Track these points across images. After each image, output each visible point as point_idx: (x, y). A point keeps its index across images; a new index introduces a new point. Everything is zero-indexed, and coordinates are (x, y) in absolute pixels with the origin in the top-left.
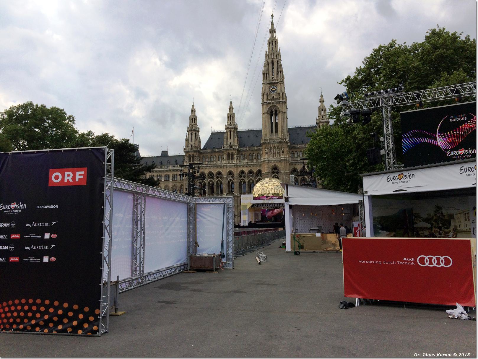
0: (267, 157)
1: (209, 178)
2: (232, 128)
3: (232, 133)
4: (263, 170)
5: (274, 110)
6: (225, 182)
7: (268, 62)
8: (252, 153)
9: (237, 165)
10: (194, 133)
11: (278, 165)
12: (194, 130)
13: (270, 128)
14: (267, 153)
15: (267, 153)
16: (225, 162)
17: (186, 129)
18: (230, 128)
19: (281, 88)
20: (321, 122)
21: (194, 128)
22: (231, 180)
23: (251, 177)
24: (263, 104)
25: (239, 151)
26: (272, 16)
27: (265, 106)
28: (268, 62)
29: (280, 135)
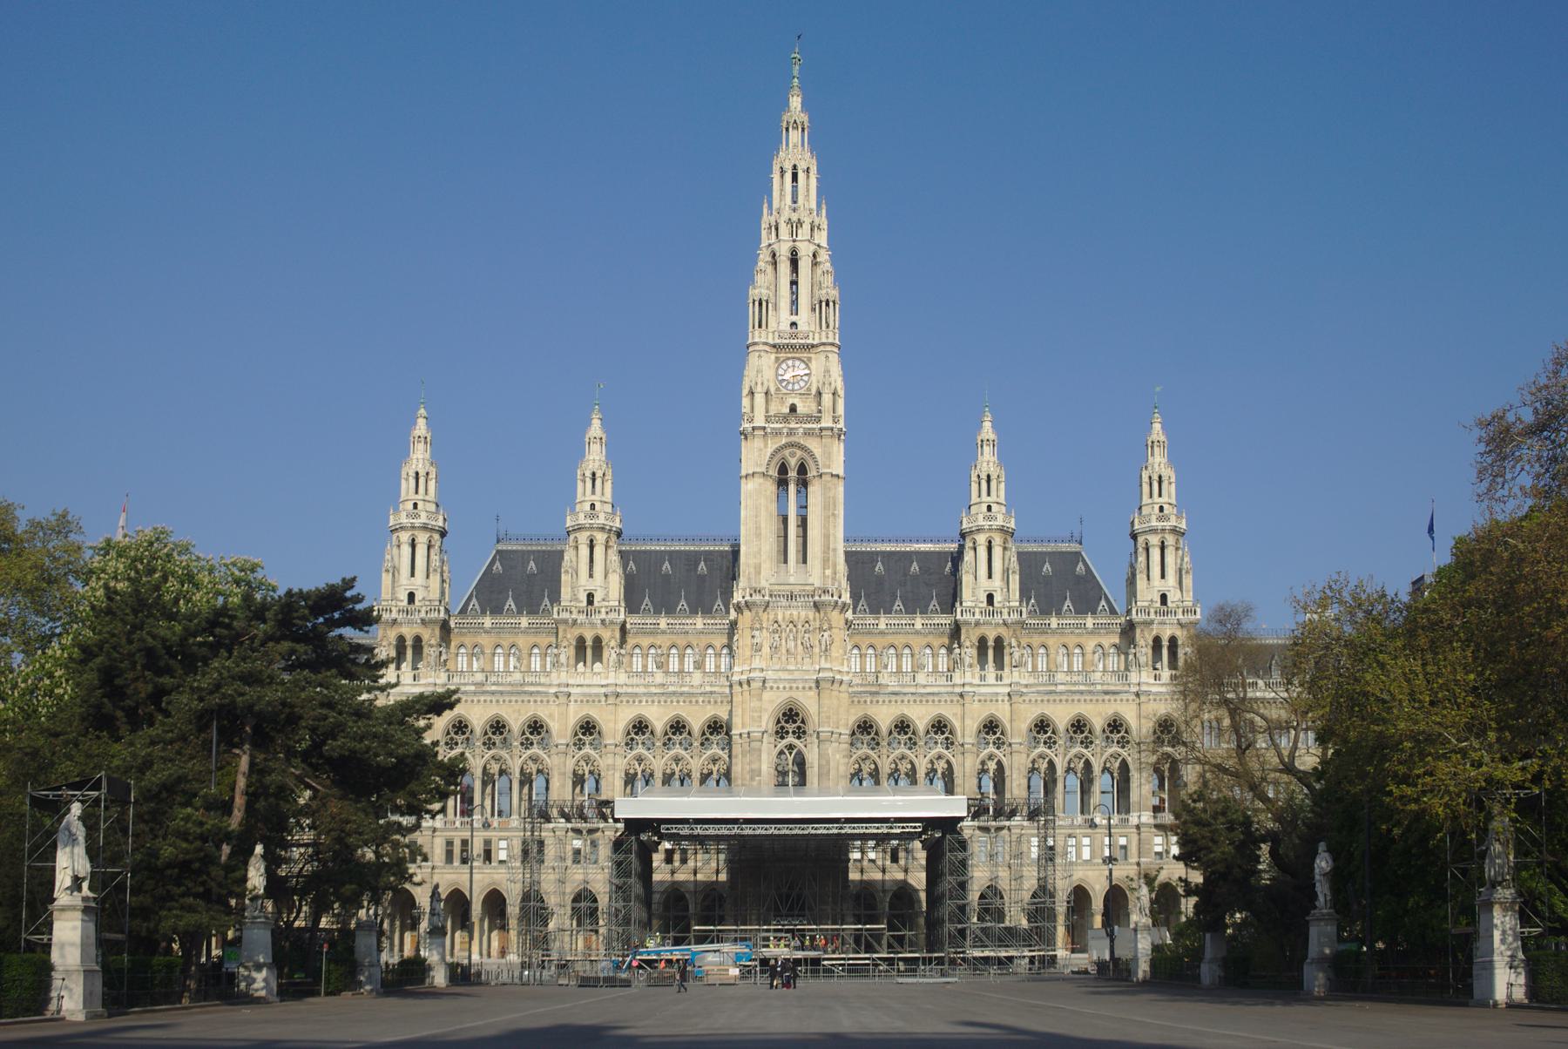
1: (489, 744)
2: (602, 529)
4: (737, 721)
5: (793, 463)
8: (681, 641)
9: (618, 695)
11: (808, 702)
18: (591, 528)
25: (623, 630)
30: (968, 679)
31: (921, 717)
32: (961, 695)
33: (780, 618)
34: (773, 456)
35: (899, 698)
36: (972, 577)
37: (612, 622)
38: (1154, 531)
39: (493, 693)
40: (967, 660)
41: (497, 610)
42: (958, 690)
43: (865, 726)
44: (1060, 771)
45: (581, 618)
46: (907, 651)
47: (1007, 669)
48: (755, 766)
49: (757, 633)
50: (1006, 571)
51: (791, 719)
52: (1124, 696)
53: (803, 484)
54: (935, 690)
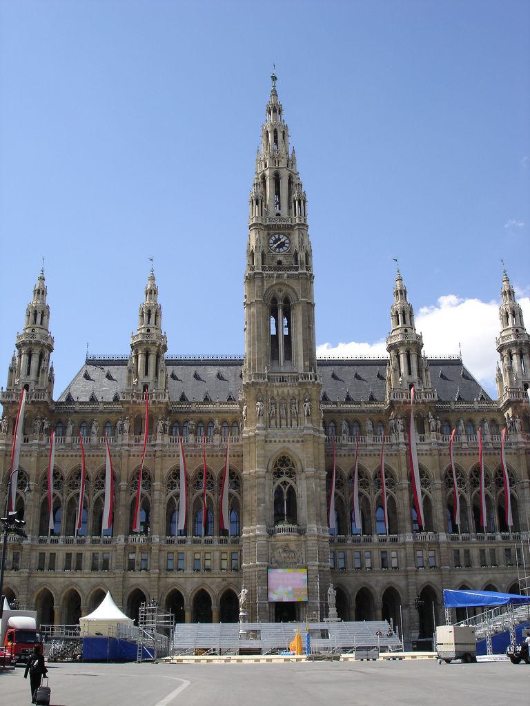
3: (152, 359)
4: (246, 464)
5: (281, 295)
7: (264, 177)
8: (205, 418)
10: (36, 351)
12: (37, 343)
13: (269, 344)
17: (15, 341)
19: (301, 241)
20: (402, 343)
21: (38, 338)
24: (250, 279)
25: (169, 413)
26: (274, 78)
27: (258, 283)
28: (264, 177)
29: (300, 363)
31: (370, 466)
33: (275, 392)
34: (267, 290)
36: (398, 373)
37: (159, 402)
38: (515, 344)
46: (356, 424)
47: (427, 434)
48: (261, 496)
49: (258, 403)
50: (419, 371)
51: (283, 466)
53: (287, 314)
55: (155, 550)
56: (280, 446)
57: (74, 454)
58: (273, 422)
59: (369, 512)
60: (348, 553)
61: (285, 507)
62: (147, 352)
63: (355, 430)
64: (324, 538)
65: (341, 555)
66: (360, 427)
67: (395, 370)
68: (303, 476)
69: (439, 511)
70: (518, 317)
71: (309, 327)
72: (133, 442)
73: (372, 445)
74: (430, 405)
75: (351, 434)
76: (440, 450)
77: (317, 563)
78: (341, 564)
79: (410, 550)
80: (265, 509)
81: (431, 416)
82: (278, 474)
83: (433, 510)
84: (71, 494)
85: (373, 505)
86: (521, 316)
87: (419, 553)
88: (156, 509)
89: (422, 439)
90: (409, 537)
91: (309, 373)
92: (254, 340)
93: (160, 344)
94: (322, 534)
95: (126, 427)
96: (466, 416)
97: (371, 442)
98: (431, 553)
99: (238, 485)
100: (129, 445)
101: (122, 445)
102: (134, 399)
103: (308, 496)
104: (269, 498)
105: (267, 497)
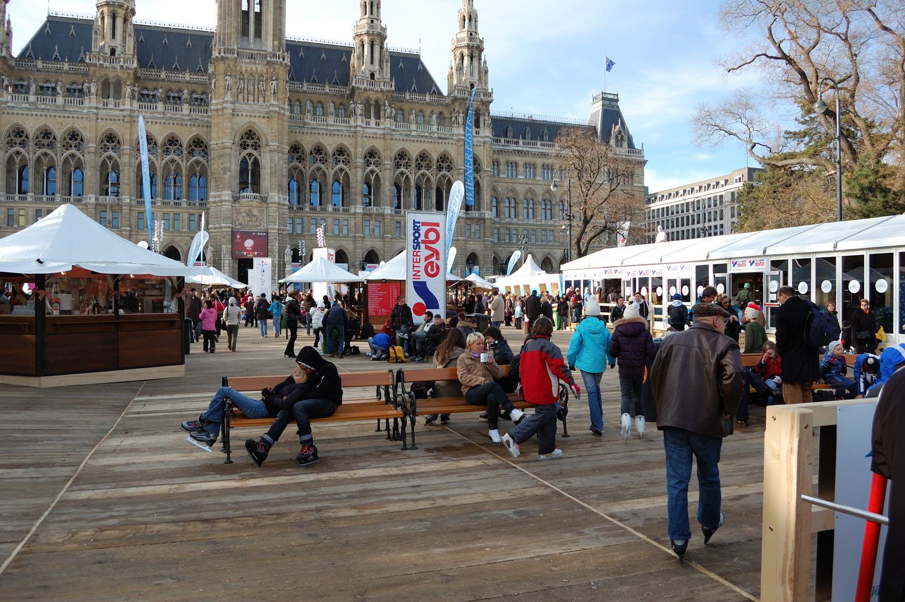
0: (229, 97)
1: (39, 145)
4: (214, 135)
6: (91, 160)
13: (239, 19)
14: (228, 88)
15: (228, 88)
16: (94, 104)
22: (110, 158)
23: (172, 156)
29: (269, 43)
30: (359, 123)
31: (330, 145)
32: (355, 132)
33: (244, 69)
35: (316, 131)
37: (128, 68)
39: (43, 110)
40: (359, 111)
41: (46, 58)
42: (352, 129)
43: (295, 149)
44: (413, 183)
45: (106, 64)
46: (320, 105)
47: (382, 120)
48: (226, 165)
50: (381, 61)
51: (249, 139)
52: (450, 141)
54: (339, 128)
55: (126, 209)
56: (247, 120)
57: (39, 113)
58: (241, 97)
59: (326, 185)
60: (306, 219)
61: (249, 176)
62: (114, 14)
63: (319, 111)
64: (284, 205)
65: (299, 221)
66: (323, 108)
67: (359, 58)
68: (267, 149)
69: (387, 188)
70: (473, 21)
71: (280, 8)
72: (100, 106)
73: (333, 126)
74: (389, 94)
75: (315, 114)
76: (392, 135)
77: (277, 227)
78: (299, 232)
79: (359, 219)
80: (231, 176)
81: (387, 104)
82: (244, 146)
83: (382, 186)
84: (39, 152)
85: (330, 180)
86: (476, 21)
87: (367, 223)
88: (126, 172)
89: (378, 124)
90: (359, 209)
91: (278, 53)
92: (225, 14)
93: (128, 8)
94: (282, 202)
95: (93, 90)
96: (418, 107)
97: (332, 123)
98: (377, 224)
99: (206, 154)
100: (97, 108)
101: (90, 108)
102: (101, 62)
103: (271, 168)
104: (235, 168)
105: (233, 167)
